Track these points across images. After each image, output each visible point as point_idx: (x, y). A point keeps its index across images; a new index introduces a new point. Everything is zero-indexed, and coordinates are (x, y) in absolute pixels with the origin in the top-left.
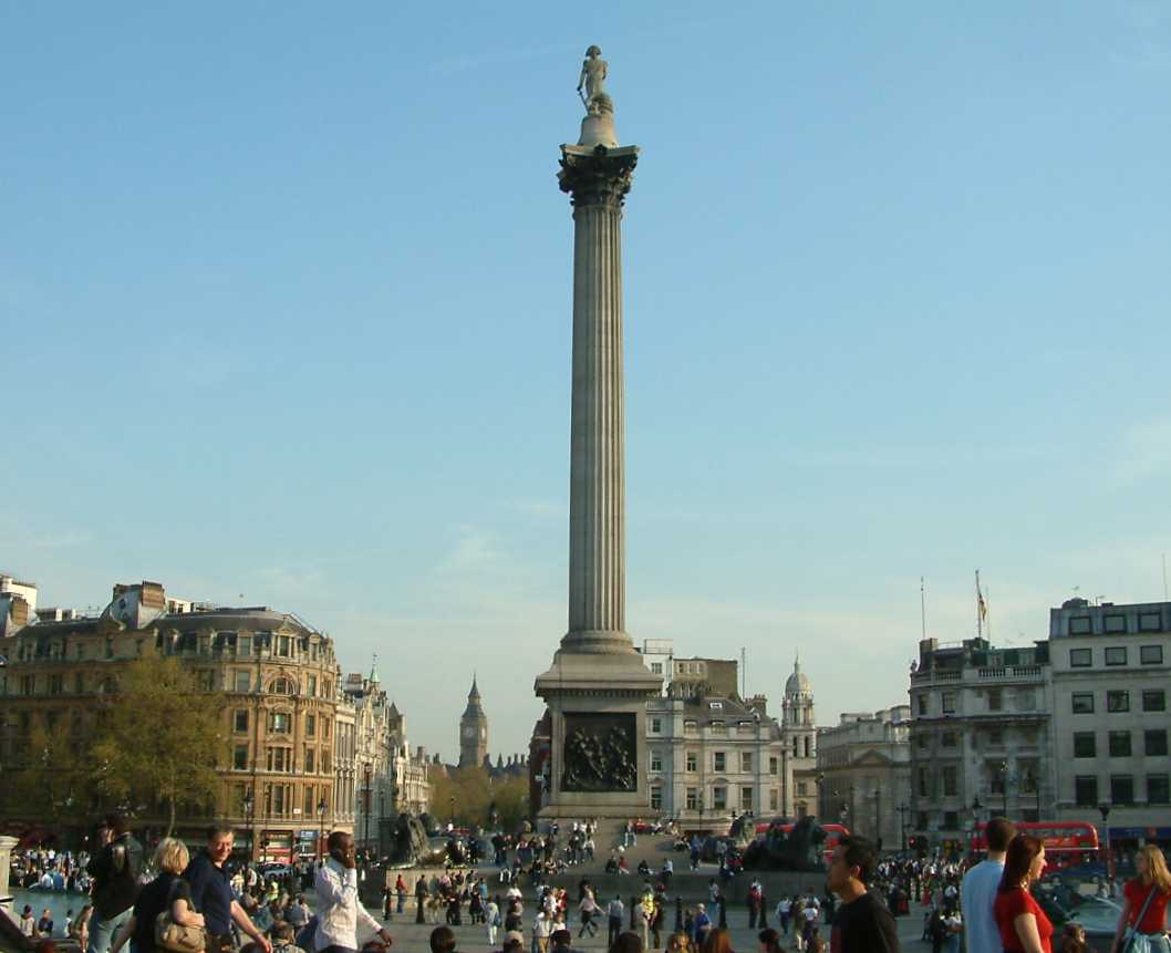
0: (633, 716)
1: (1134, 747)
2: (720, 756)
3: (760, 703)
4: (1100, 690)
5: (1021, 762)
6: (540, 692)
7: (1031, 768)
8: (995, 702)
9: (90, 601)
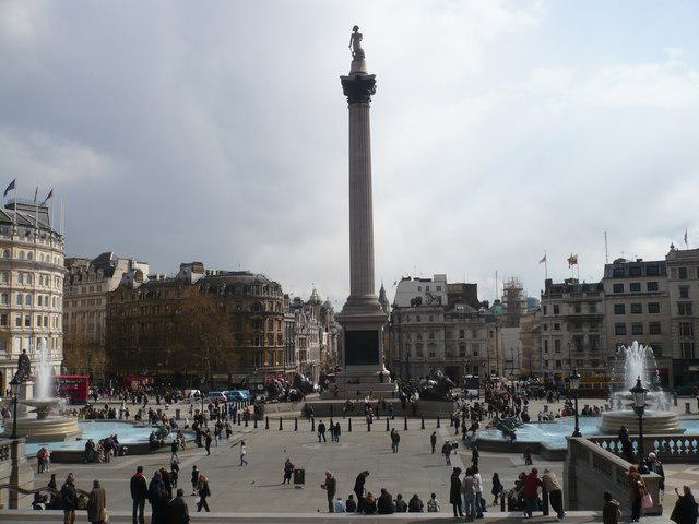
0: (377, 331)
1: (644, 332)
2: (462, 332)
3: (486, 304)
5: (590, 336)
7: (594, 339)
8: (578, 310)
9: (170, 271)
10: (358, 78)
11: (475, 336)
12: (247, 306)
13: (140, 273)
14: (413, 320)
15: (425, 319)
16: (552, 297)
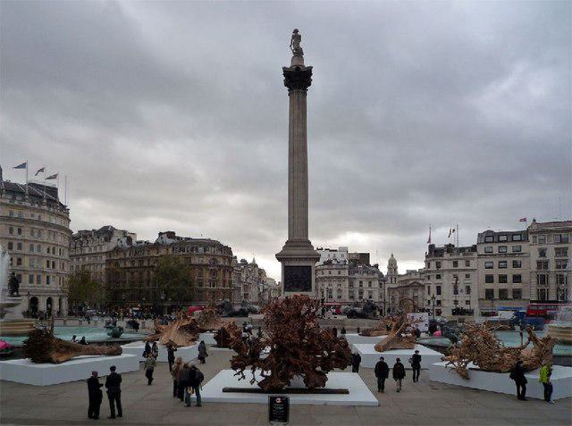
2: (361, 282)
4: (496, 261)
6: (279, 259)
8: (455, 264)
9: (153, 238)
10: (298, 68)
11: (370, 286)
12: (206, 261)
13: (129, 240)
14: (326, 274)
15: (335, 273)
16: (436, 256)
